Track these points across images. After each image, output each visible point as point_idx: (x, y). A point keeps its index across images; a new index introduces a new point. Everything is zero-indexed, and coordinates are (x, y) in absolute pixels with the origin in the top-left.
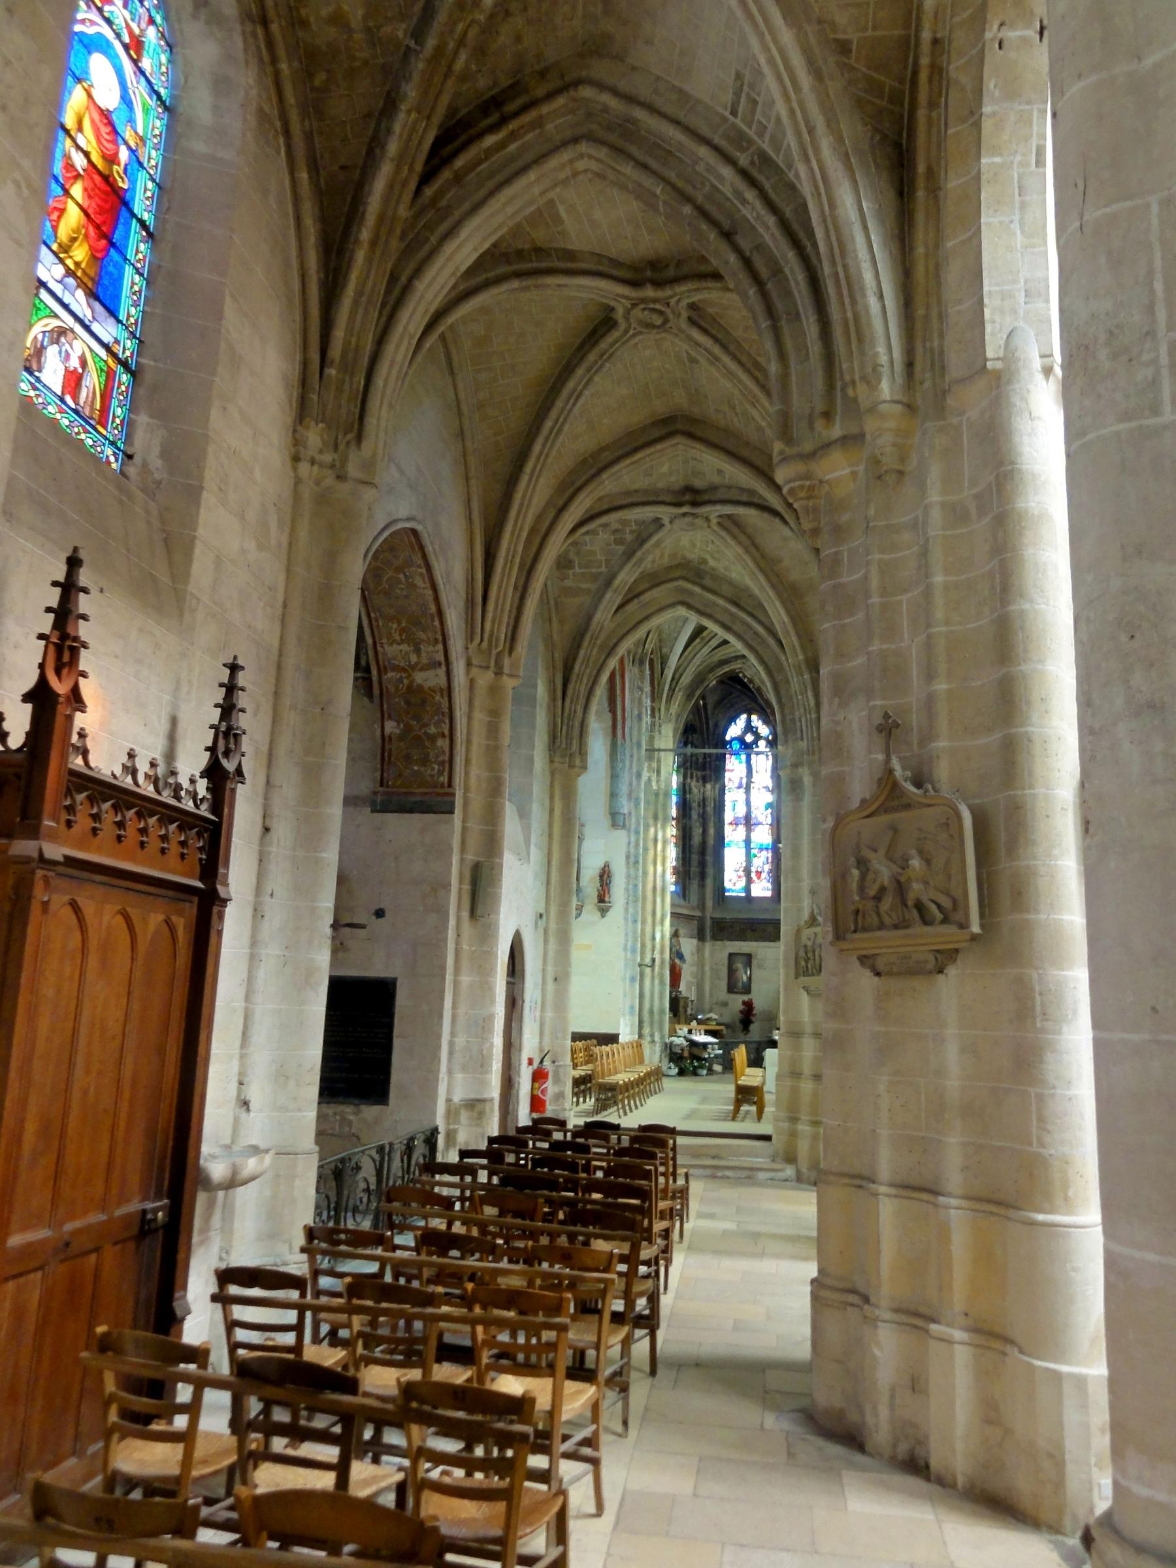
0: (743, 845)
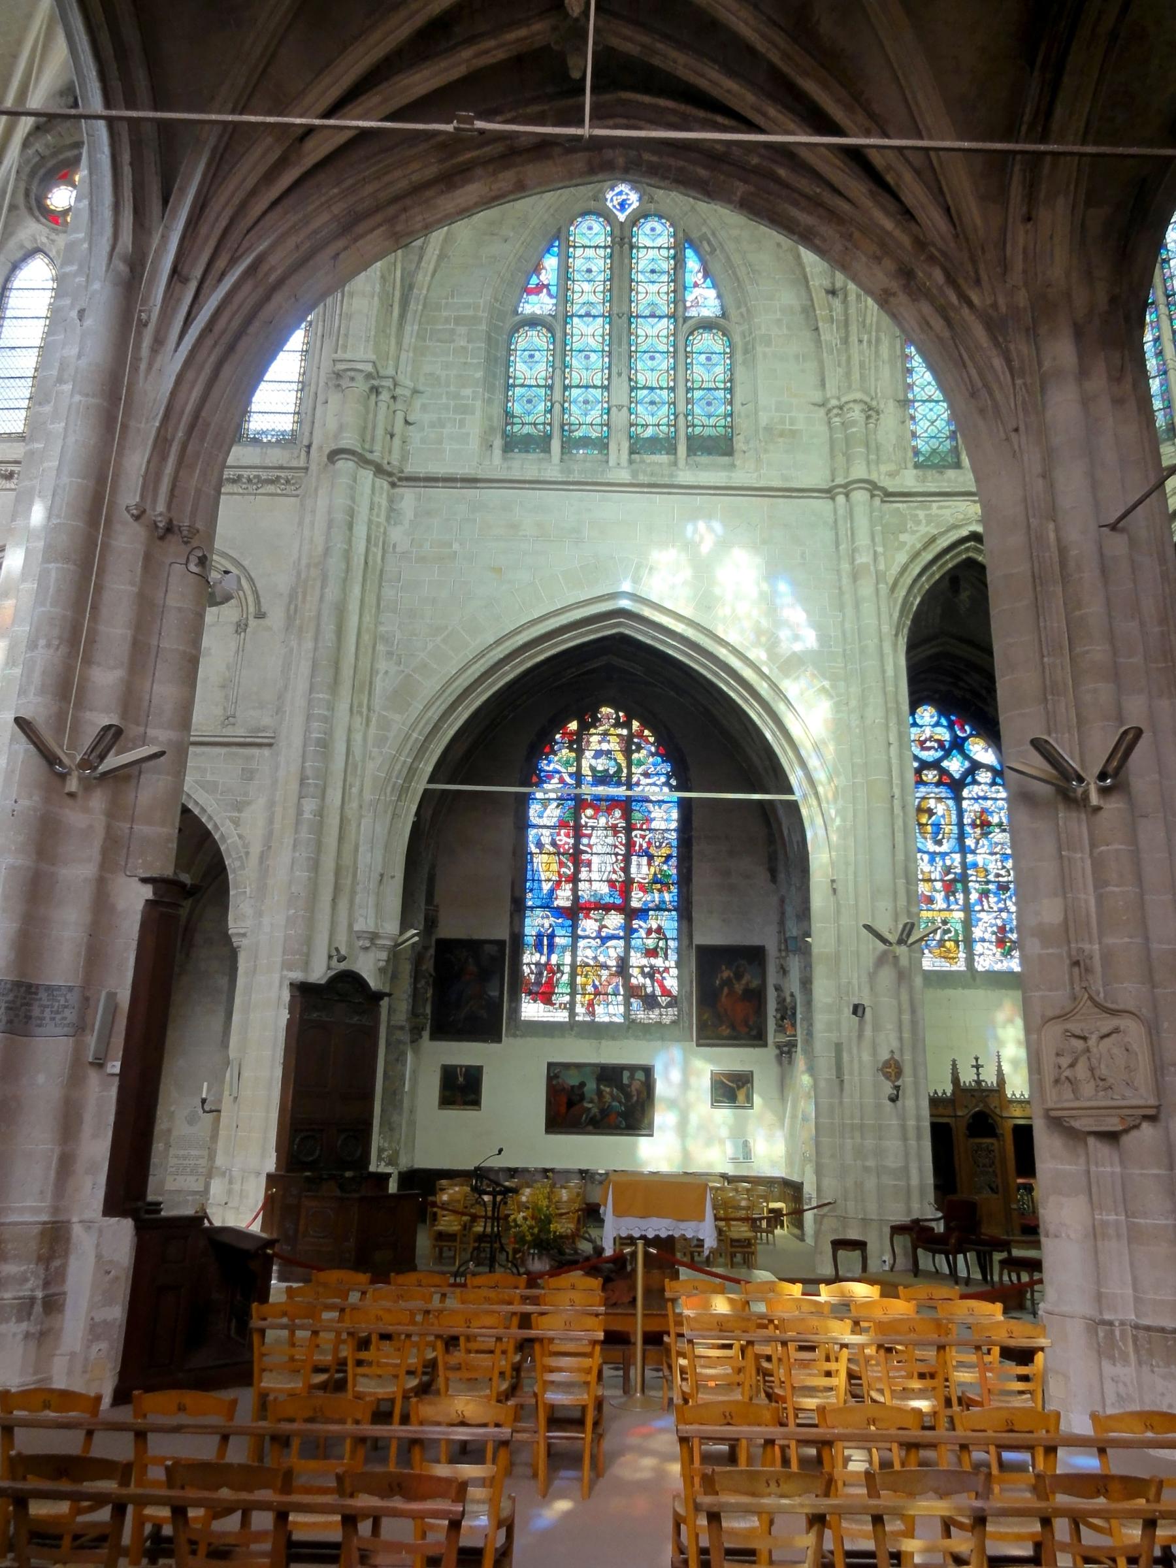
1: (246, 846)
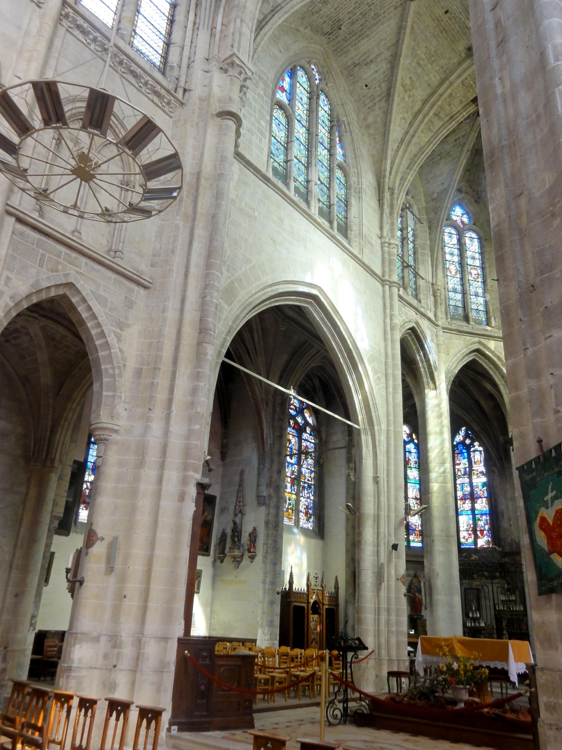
0: (470, 512)
1: (124, 359)
